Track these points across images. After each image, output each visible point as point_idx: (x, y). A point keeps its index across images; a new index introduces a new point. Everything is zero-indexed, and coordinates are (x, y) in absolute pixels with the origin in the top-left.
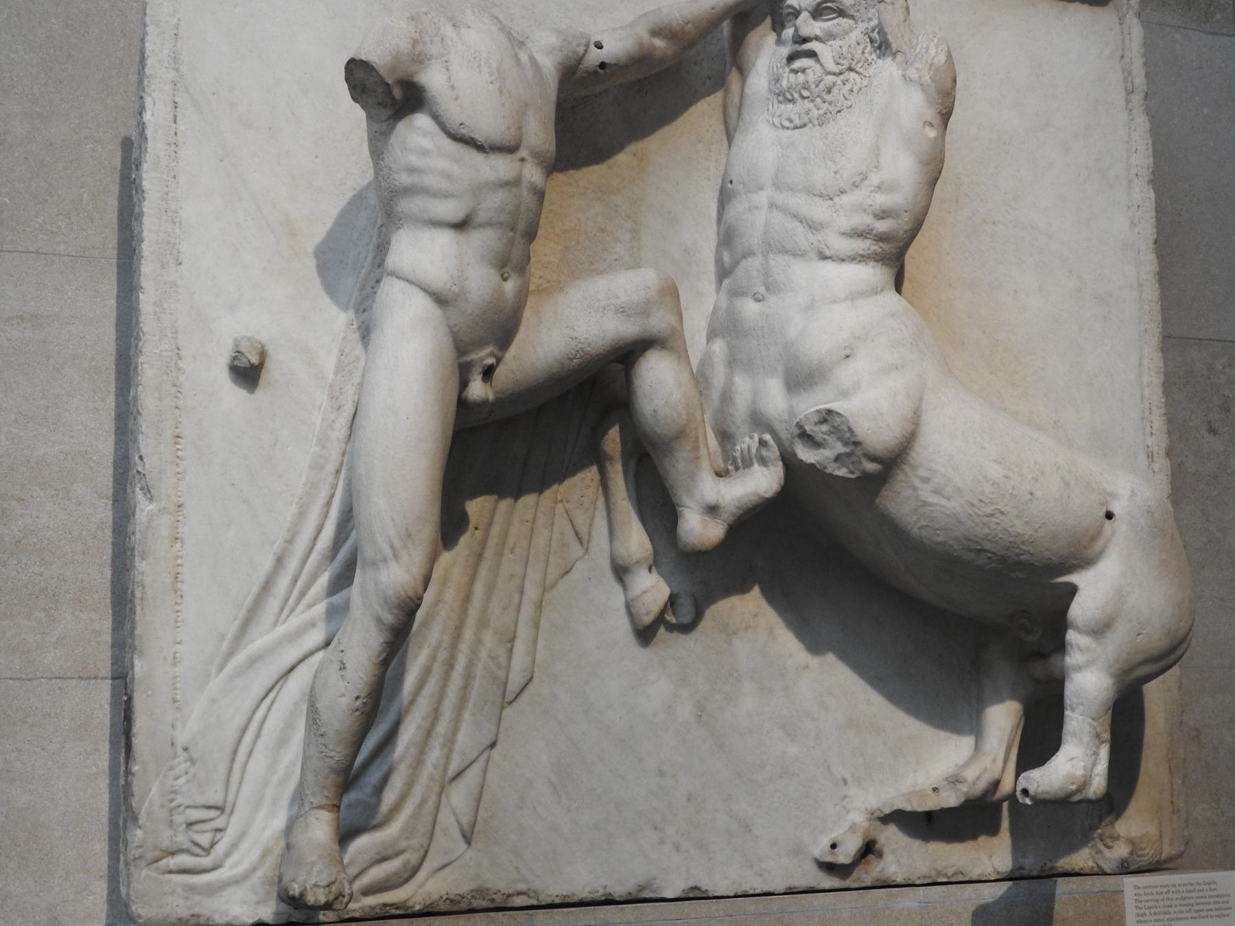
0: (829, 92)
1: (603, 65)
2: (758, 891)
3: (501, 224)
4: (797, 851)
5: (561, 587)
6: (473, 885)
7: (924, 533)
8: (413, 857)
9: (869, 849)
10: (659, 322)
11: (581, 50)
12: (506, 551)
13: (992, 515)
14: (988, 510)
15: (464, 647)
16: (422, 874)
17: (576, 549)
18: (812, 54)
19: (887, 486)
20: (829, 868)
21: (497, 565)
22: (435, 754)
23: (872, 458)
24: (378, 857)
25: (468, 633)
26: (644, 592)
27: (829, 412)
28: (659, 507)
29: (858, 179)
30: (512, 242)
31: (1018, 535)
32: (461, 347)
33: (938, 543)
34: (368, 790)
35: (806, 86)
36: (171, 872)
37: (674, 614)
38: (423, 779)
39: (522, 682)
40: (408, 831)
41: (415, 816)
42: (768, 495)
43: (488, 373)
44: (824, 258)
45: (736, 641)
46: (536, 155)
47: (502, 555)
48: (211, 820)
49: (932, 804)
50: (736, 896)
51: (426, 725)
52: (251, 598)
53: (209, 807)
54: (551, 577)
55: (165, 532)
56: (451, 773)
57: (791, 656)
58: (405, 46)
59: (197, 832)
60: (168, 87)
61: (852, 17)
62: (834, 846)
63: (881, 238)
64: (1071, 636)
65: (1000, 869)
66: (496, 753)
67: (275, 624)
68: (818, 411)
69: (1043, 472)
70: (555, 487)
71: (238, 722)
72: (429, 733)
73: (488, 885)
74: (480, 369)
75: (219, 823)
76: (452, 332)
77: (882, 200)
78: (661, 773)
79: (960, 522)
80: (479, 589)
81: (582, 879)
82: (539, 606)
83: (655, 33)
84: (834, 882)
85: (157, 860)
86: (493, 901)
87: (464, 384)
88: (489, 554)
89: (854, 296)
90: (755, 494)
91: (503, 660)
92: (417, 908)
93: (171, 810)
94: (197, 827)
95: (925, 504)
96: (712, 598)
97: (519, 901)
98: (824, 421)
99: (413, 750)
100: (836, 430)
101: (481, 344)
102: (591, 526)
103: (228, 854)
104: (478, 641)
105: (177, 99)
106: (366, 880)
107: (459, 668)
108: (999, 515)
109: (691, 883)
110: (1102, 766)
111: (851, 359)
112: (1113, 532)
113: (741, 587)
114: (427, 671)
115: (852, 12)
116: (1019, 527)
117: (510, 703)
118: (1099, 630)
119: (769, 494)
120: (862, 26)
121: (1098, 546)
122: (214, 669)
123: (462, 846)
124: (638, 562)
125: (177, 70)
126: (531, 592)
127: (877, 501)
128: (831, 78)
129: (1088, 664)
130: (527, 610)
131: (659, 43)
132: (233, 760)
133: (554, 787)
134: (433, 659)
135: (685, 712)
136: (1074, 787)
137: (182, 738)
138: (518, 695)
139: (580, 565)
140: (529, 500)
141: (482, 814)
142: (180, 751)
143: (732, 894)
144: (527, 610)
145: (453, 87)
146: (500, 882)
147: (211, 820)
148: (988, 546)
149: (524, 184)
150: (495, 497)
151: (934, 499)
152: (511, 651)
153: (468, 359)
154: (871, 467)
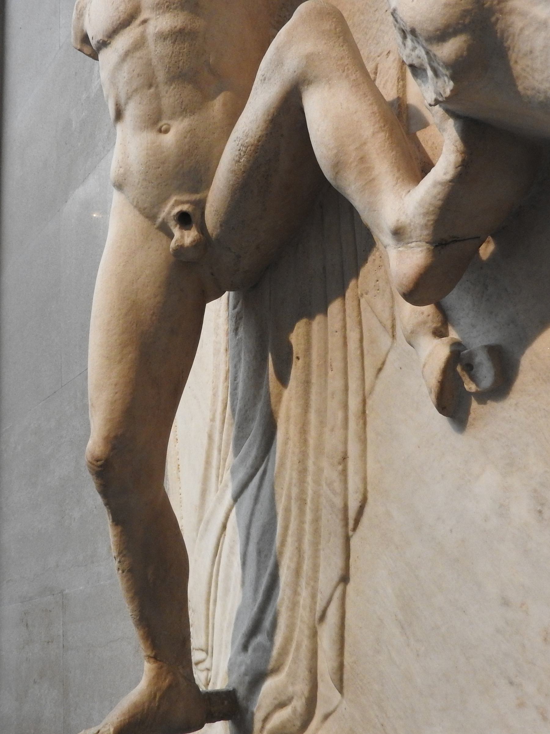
3: (136, 90)
8: (298, 704)
12: (329, 370)
15: (309, 479)
17: (385, 340)
19: (513, 56)
21: (324, 387)
24: (276, 702)
30: (157, 97)
32: (149, 213)
37: (473, 379)
38: (299, 623)
40: (292, 676)
41: (294, 661)
42: (449, 177)
43: (184, 219)
47: (326, 374)
51: (293, 566)
56: (318, 614)
66: (350, 588)
70: (352, 284)
72: (297, 572)
76: (136, 207)
78: (506, 603)
80: (313, 417)
88: (314, 379)
91: (337, 486)
96: (525, 339)
101: (162, 200)
102: (392, 307)
104: (319, 470)
114: (288, 510)
117: (354, 529)
123: (339, 695)
124: (412, 332)
127: (520, 88)
133: (402, 628)
134: (289, 497)
135: (521, 510)
138: (357, 521)
139: (392, 357)
140: (334, 308)
149: (151, 40)
152: (344, 473)
153: (160, 220)
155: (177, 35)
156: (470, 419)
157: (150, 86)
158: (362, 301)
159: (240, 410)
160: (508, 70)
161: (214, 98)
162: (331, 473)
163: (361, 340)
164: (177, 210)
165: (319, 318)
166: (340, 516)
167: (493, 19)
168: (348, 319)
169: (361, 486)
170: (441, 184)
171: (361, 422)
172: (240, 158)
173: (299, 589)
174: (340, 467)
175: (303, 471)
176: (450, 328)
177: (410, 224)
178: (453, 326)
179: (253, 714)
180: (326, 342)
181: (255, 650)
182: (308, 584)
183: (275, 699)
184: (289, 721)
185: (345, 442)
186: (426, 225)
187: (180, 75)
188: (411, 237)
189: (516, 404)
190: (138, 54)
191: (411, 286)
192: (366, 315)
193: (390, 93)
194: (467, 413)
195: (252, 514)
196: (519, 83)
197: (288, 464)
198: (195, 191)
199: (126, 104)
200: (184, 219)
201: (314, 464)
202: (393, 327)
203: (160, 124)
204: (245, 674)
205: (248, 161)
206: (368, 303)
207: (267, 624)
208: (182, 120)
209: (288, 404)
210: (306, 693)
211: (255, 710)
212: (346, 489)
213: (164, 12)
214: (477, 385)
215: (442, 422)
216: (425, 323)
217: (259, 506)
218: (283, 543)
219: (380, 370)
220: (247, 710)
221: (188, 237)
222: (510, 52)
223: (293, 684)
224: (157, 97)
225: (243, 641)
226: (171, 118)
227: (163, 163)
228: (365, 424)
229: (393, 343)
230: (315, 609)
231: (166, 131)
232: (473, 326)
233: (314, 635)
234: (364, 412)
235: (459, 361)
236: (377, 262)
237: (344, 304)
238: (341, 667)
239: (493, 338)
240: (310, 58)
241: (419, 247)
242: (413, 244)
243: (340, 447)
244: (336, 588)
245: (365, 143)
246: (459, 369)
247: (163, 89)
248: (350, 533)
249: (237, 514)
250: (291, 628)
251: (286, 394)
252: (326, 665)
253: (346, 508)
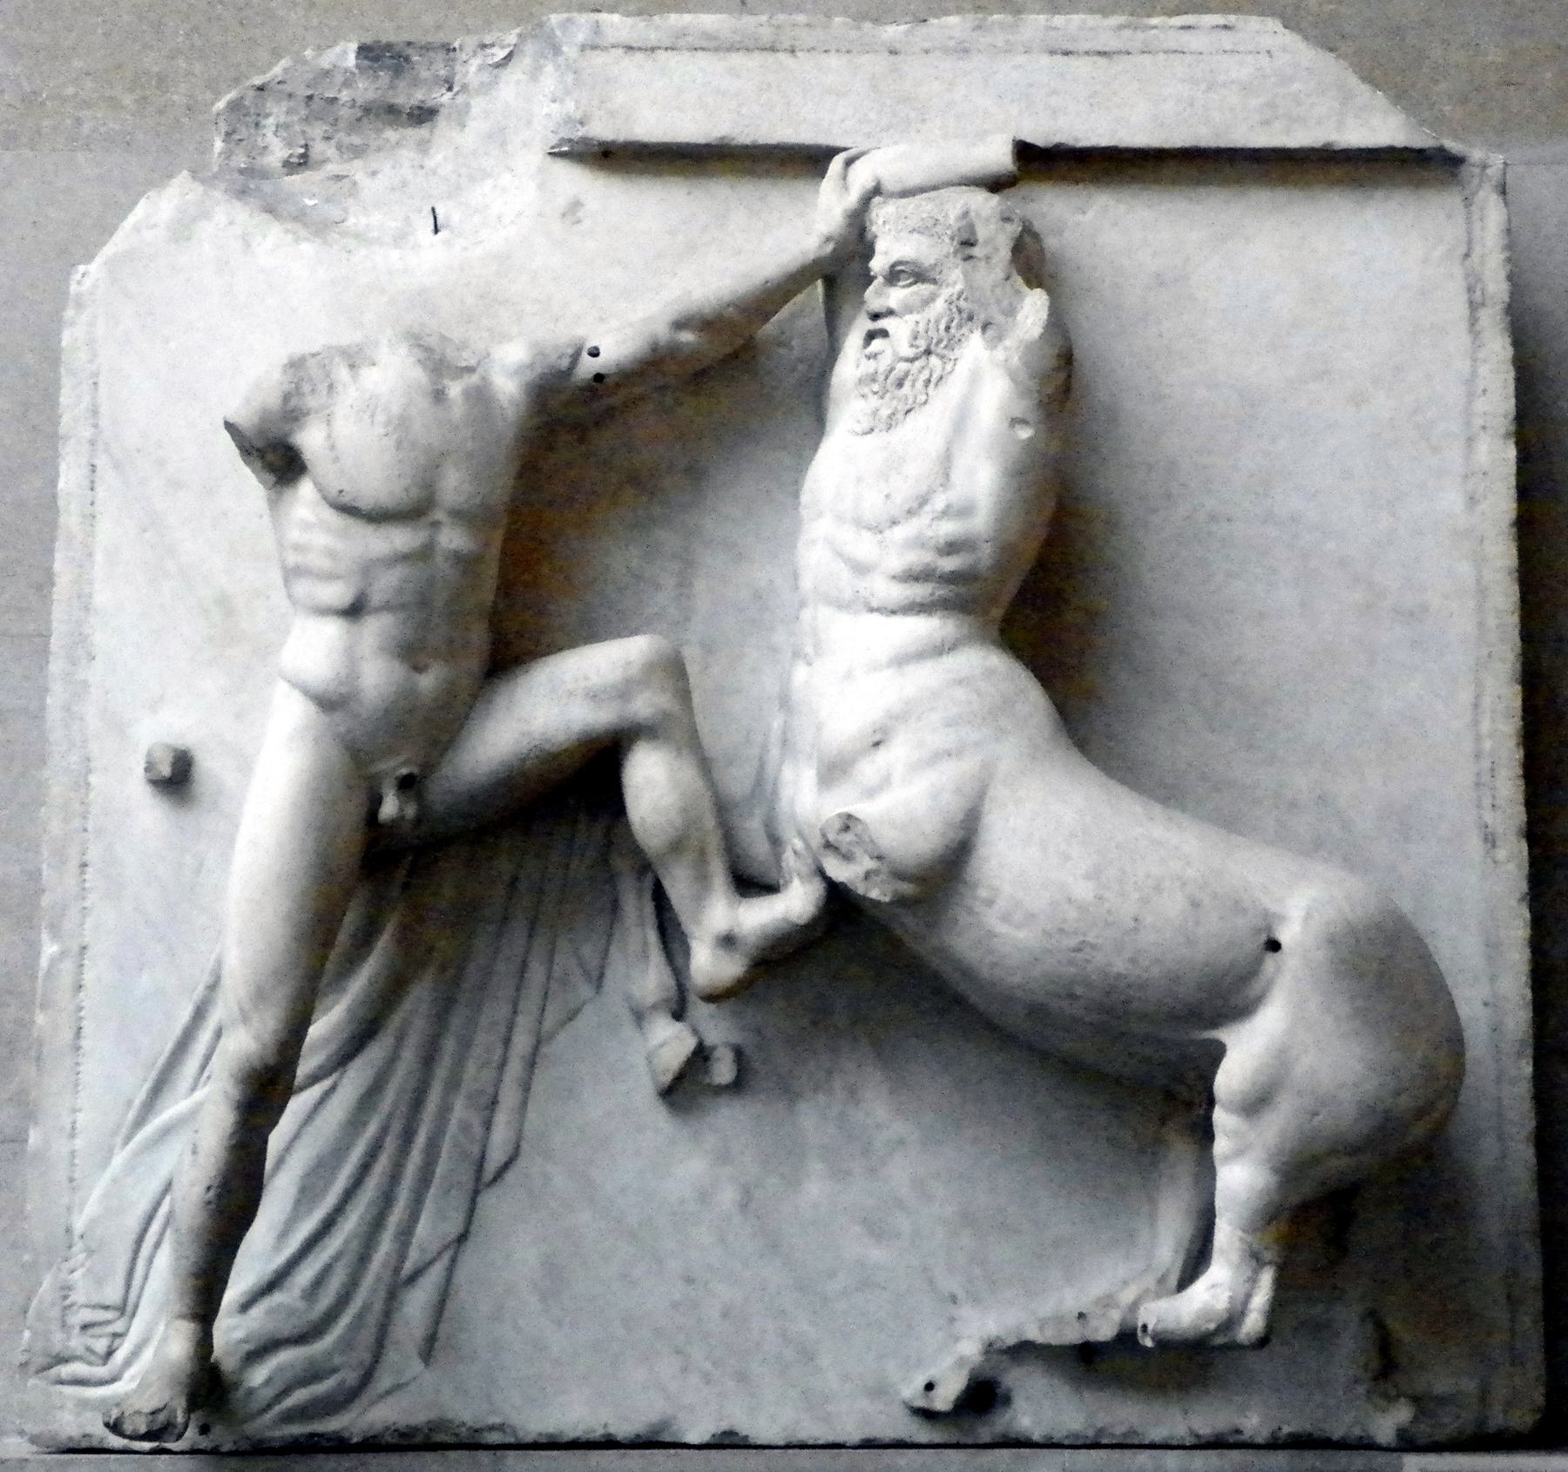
0: (900, 384)
1: (599, 377)
2: (821, 1442)
4: (880, 1391)
5: (562, 1037)
6: (432, 1415)
8: (351, 1377)
9: (982, 1396)
10: (643, 706)
11: (565, 363)
13: (1078, 950)
14: (1073, 942)
16: (365, 1398)
17: (585, 990)
18: (884, 333)
20: (927, 1415)
26: (661, 1046)
27: (849, 817)
28: (671, 934)
29: (915, 505)
31: (1119, 976)
34: (297, 1292)
35: (873, 378)
36: (62, 1382)
39: (504, 1159)
40: (346, 1343)
43: (407, 785)
44: (872, 610)
46: (458, 515)
48: (108, 1322)
49: (1072, 1335)
50: (788, 1447)
52: (162, 1060)
53: (106, 1308)
54: (548, 1024)
55: (66, 978)
58: (274, 401)
59: (93, 1336)
60: (86, 447)
61: (934, 282)
62: (929, 1387)
63: (952, 578)
64: (1220, 1117)
65: (1201, 1432)
67: (193, 1089)
68: (839, 815)
69: (1158, 889)
71: (143, 1206)
73: (450, 1416)
74: (394, 782)
75: (118, 1327)
77: (948, 529)
80: (449, 1045)
81: (574, 1414)
82: (531, 1064)
83: (679, 325)
84: (923, 1433)
85: (50, 1367)
86: (457, 1435)
87: (376, 801)
89: (903, 660)
90: (785, 920)
91: (478, 1130)
92: (355, 1440)
93: (66, 1308)
94: (91, 1331)
95: (991, 934)
97: (494, 1438)
98: (847, 828)
99: (355, 1245)
100: (859, 841)
101: (390, 751)
103: (128, 1363)
104: (445, 1111)
105: (96, 462)
106: (289, 1402)
107: (421, 1139)
108: (1088, 950)
109: (724, 1426)
110: (1261, 1298)
111: (881, 747)
112: (1278, 970)
115: (933, 274)
116: (1120, 966)
118: (1255, 1104)
119: (802, 922)
120: (946, 293)
121: (1255, 988)
122: (119, 1140)
125: (96, 426)
126: (522, 1042)
128: (902, 366)
129: (1238, 1154)
130: (515, 1068)
131: (687, 337)
132: (136, 1252)
134: (385, 1129)
136: (1212, 1326)
137: (79, 1225)
139: (588, 1011)
142: (76, 1239)
143: (782, 1443)
144: (515, 1068)
145: (332, 447)
146: (466, 1412)
147: (108, 1322)
151: (1002, 928)
154: (907, 888)
164: (404, 771)
175: (417, 1104)
181: (270, 1312)
185: (498, 1082)
204: (245, 1341)
210: (367, 1364)
217: (310, 1129)
220: (237, 1385)
240: (667, 715)
243: (490, 1090)
244: (446, 1247)
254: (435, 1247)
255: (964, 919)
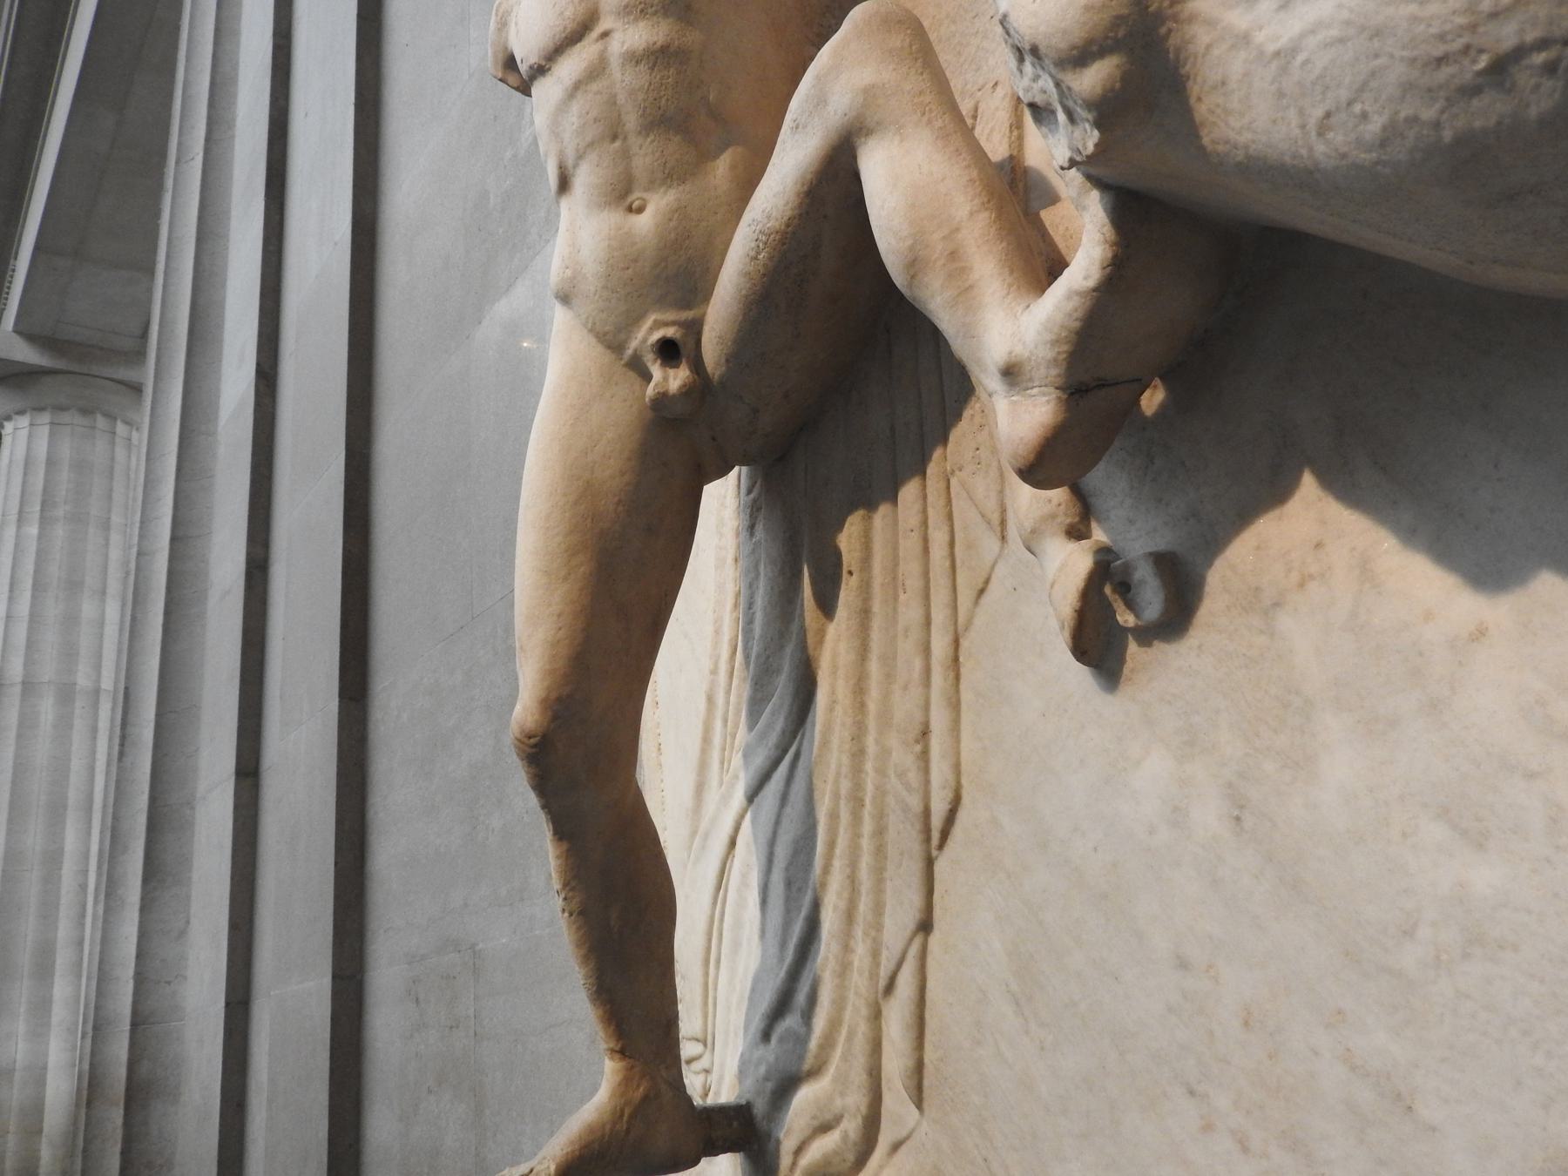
3: (591, 145)
5: (980, 619)
7: (1338, 138)
8: (851, 1126)
12: (901, 591)
15: (869, 766)
17: (990, 544)
19: (1194, 89)
21: (892, 619)
22: (861, 950)
23: (1080, 57)
24: (816, 1123)
25: (870, 741)
30: (626, 155)
32: (613, 341)
33: (1383, 143)
37: (1131, 606)
38: (851, 996)
40: (842, 1081)
41: (844, 1058)
42: (1091, 283)
43: (669, 351)
45: (1285, 622)
47: (896, 598)
51: (843, 905)
56: (882, 983)
57: (1428, 616)
66: (935, 940)
70: (937, 454)
72: (850, 916)
76: (591, 331)
78: (1183, 964)
79: (1378, 33)
80: (874, 666)
88: (877, 606)
91: (913, 777)
95: (1285, 55)
96: (1214, 542)
102: (1001, 492)
104: (885, 753)
113: (1276, 492)
114: (834, 816)
117: (941, 847)
124: (1033, 532)
127: (1206, 141)
134: (836, 796)
135: (1208, 816)
140: (909, 492)
141: (930, 1055)
148: (1507, 35)
150: (861, 513)
152: (925, 755)
153: (629, 352)
154: (1092, 79)
155: (658, 57)
156: (1126, 670)
157: (614, 137)
158: (954, 481)
159: (758, 656)
160: (1186, 111)
161: (716, 157)
162: (903, 757)
163: (952, 544)
164: (657, 335)
165: (884, 510)
166: (918, 826)
167: (1163, 30)
168: (930, 511)
169: (951, 778)
170: (1079, 293)
171: (952, 675)
172: (758, 253)
173: (852, 943)
174: (918, 748)
175: (858, 754)
176: (1094, 525)
177: (1029, 359)
178: (1099, 521)
179: (778, 1142)
180: (895, 548)
182: (866, 934)
183: (814, 1118)
184: (836, 1153)
186: (1055, 360)
187: (660, 121)
188: (1031, 380)
189: (1200, 647)
190: (594, 87)
191: (1032, 457)
192: (960, 505)
193: (997, 149)
194: (1121, 660)
195: (777, 823)
196: (1204, 132)
197: (835, 742)
198: (686, 305)
199: (576, 166)
200: (669, 351)
201: (877, 742)
202: (1003, 523)
203: (629, 200)
204: (766, 1079)
205: (771, 258)
206: (963, 484)
207: (801, 998)
208: (665, 193)
209: (834, 646)
210: (864, 1110)
211: (782, 1136)
212: (927, 782)
213: (636, 20)
214: (1137, 616)
215: (1080, 674)
216: (1053, 516)
217: (788, 810)
218: (826, 869)
219: (982, 591)
220: (769, 1135)
221: (676, 379)
222: (1190, 83)
223: (842, 1094)
224: (626, 155)
225: (762, 1026)
226: (647, 190)
227: (635, 261)
228: (957, 678)
229: (1002, 548)
230: (878, 975)
231: (640, 210)
232: (1131, 522)
233: (876, 1015)
234: (956, 659)
235: (1108, 575)
236: (978, 420)
237: (924, 487)
238: (919, 1067)
239: (1161, 543)
240: (869, 94)
241: (1044, 394)
242: (1035, 391)
243: (918, 716)
245: (957, 230)
246: (1108, 590)
247: (635, 142)
248: (934, 853)
249: (754, 821)
250: (839, 1004)
251: (832, 629)
252: (895, 1064)
253: (927, 813)
254: (900, 946)
255: (1237, 65)
